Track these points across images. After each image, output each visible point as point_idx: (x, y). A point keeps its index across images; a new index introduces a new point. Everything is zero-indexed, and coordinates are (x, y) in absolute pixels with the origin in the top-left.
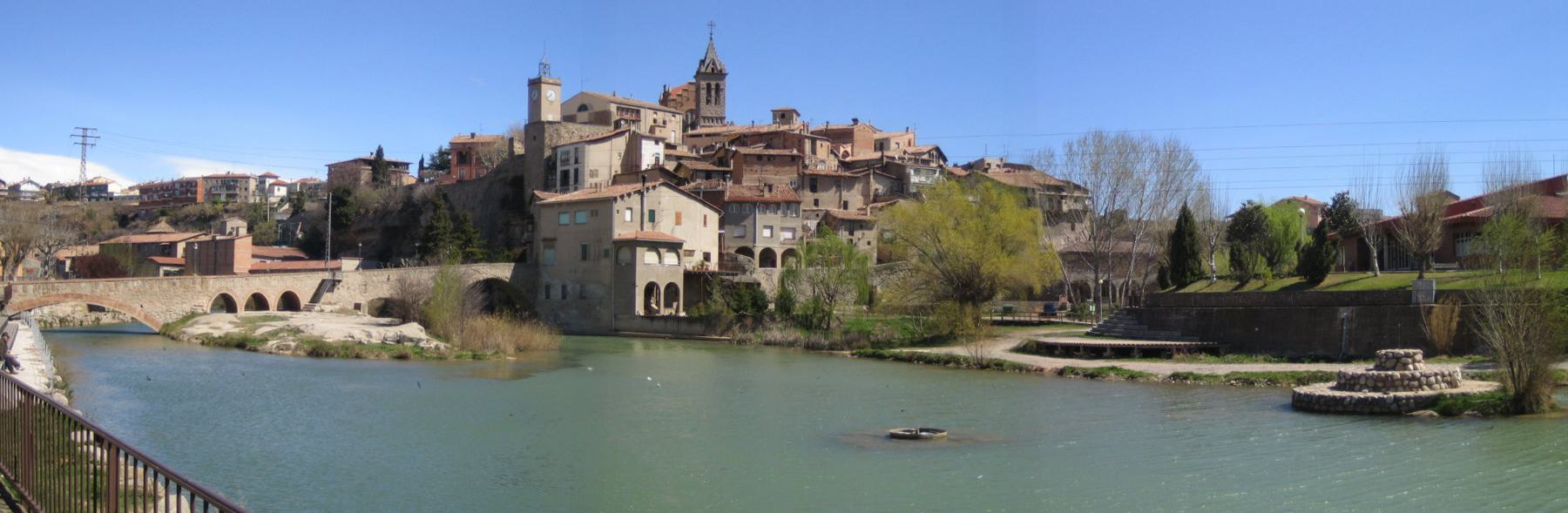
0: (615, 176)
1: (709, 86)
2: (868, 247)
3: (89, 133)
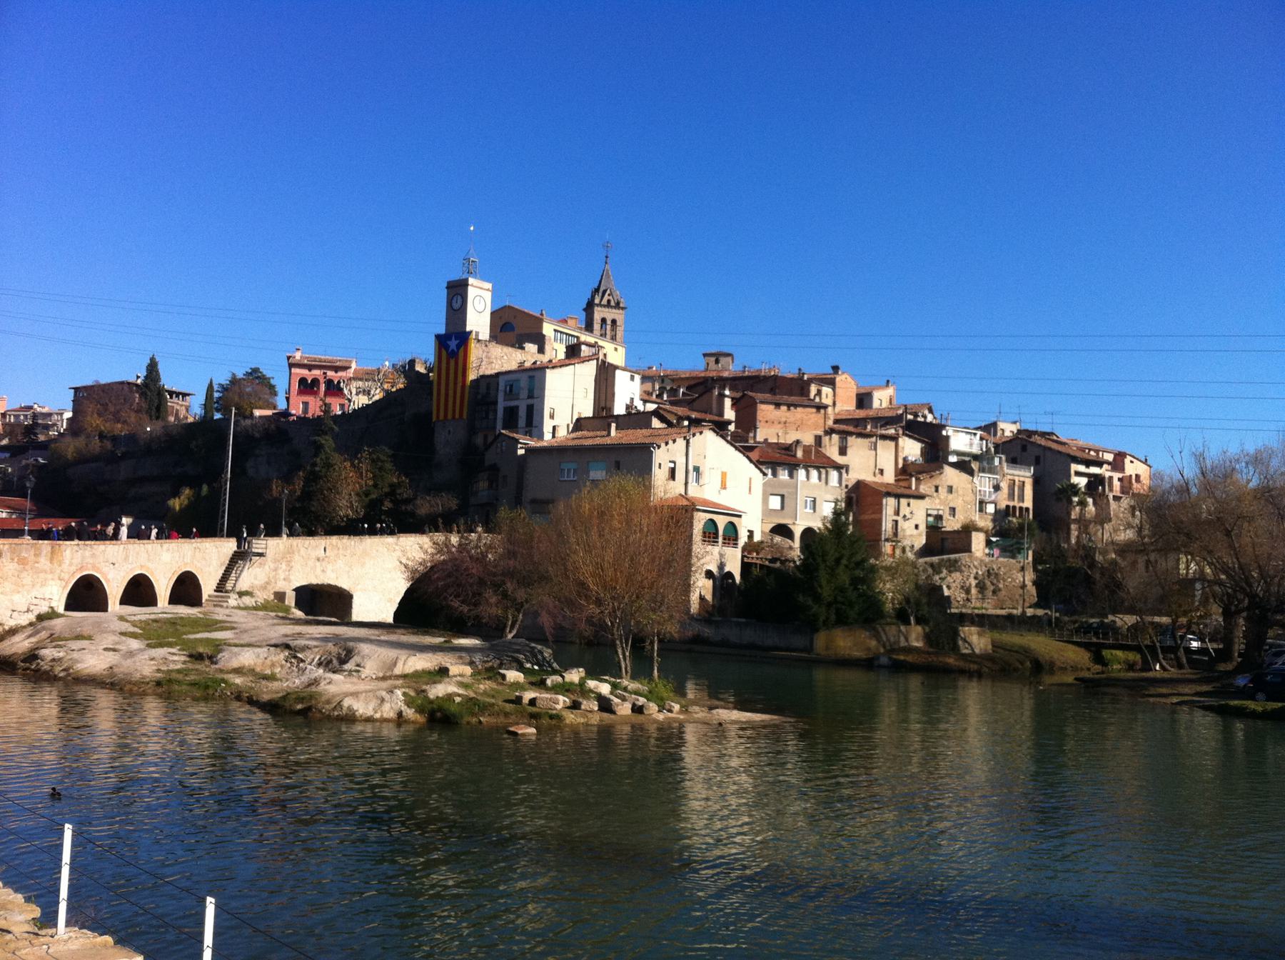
0: (579, 420)
1: (604, 321)
2: (915, 532)
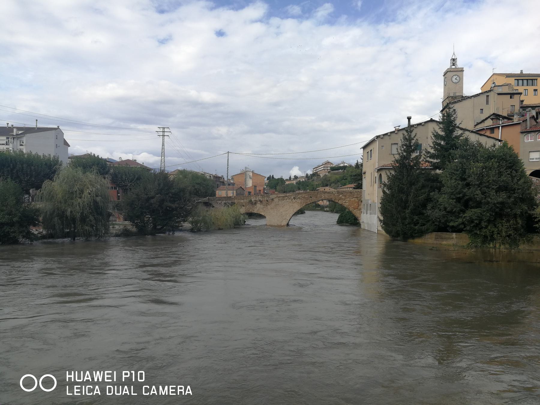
3: (166, 130)
